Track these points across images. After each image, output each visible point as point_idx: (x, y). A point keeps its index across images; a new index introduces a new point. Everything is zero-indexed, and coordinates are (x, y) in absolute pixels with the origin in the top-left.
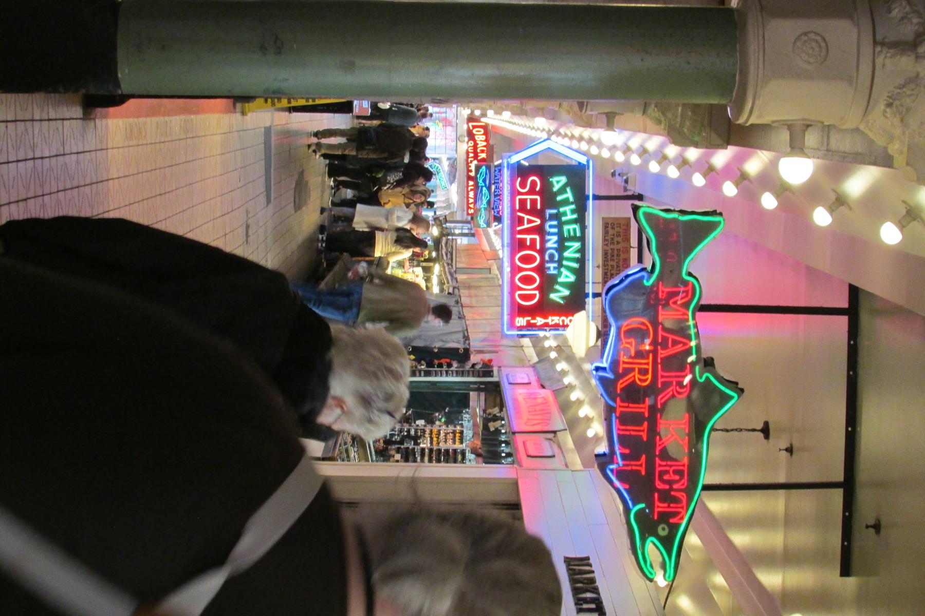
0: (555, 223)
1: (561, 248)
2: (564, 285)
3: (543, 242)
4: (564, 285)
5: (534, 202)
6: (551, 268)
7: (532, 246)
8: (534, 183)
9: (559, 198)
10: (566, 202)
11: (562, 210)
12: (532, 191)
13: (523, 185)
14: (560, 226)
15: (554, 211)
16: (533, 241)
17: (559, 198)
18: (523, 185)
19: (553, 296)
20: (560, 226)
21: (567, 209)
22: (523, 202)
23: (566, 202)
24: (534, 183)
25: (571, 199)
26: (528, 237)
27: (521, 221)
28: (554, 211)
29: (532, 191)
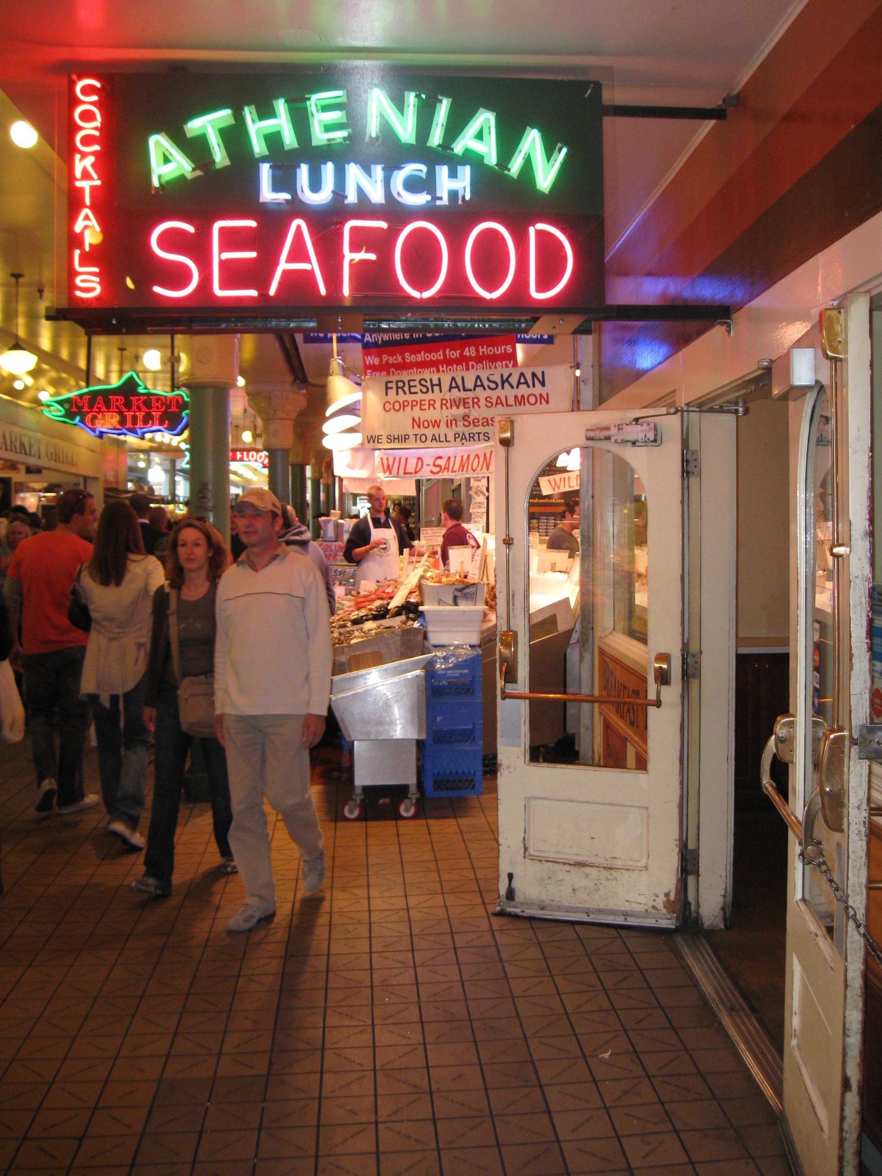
0: (303, 171)
1: (392, 155)
2: (508, 142)
3: (364, 209)
4: (508, 142)
5: (231, 240)
6: (454, 184)
7: (381, 243)
8: (171, 241)
9: (220, 156)
10: (234, 137)
11: (259, 147)
13: (179, 277)
14: (316, 157)
17: (220, 156)
18: (179, 277)
19: (546, 177)
20: (316, 157)
21: (257, 130)
22: (233, 274)
23: (234, 137)
24: (171, 241)
25: (223, 116)
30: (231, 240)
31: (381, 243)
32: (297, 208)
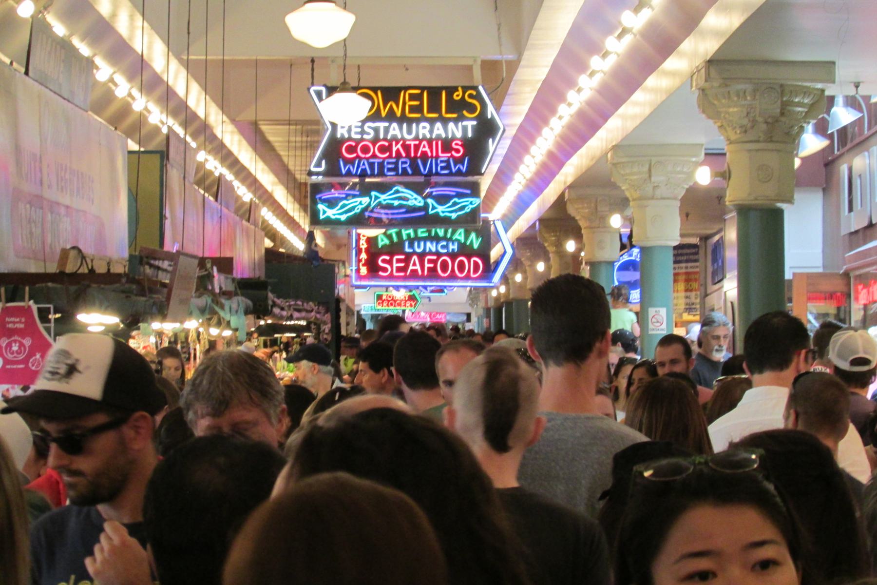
0: (416, 244)
3: (431, 253)
5: (398, 261)
7: (434, 262)
8: (384, 261)
9: (395, 239)
10: (399, 234)
11: (405, 237)
12: (390, 262)
14: (419, 239)
15: (407, 244)
16: (430, 261)
17: (395, 239)
20: (419, 239)
21: (404, 233)
22: (399, 269)
23: (399, 234)
24: (384, 261)
25: (396, 230)
26: (427, 265)
27: (414, 271)
28: (407, 244)
29: (390, 262)
30: (398, 261)
31: (434, 262)
32: (414, 253)
